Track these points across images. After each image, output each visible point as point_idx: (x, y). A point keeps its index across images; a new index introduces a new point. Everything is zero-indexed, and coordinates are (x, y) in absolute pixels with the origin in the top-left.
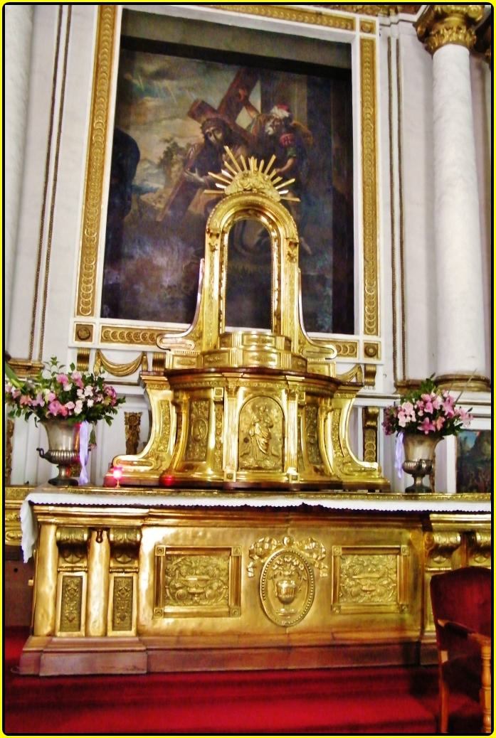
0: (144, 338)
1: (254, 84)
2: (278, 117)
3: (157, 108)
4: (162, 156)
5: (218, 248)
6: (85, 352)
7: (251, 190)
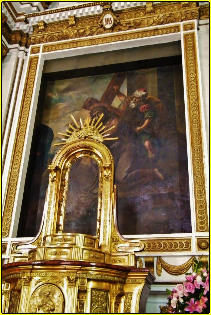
1: (122, 82)
2: (138, 96)
3: (65, 108)
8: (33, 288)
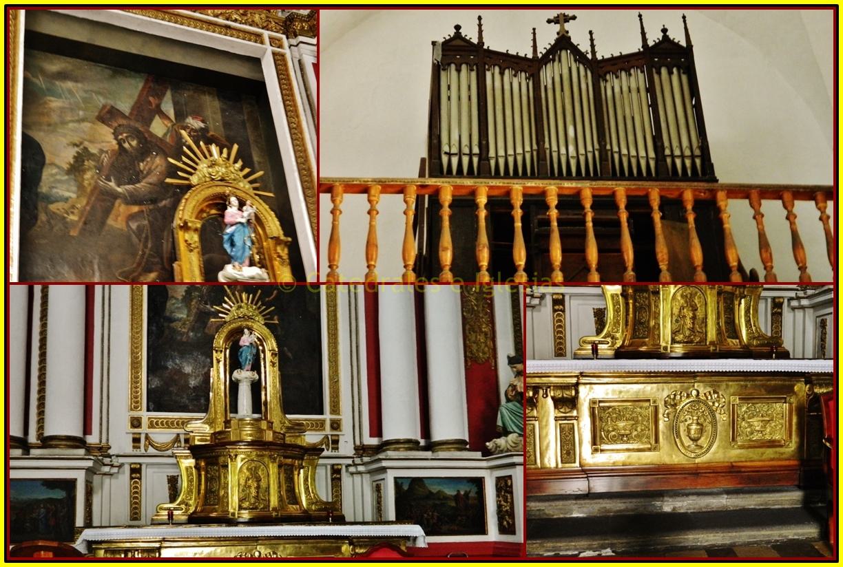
0: (178, 424)
4: (184, 294)
5: (223, 359)
6: (138, 436)
7: (243, 317)
8: (239, 464)
